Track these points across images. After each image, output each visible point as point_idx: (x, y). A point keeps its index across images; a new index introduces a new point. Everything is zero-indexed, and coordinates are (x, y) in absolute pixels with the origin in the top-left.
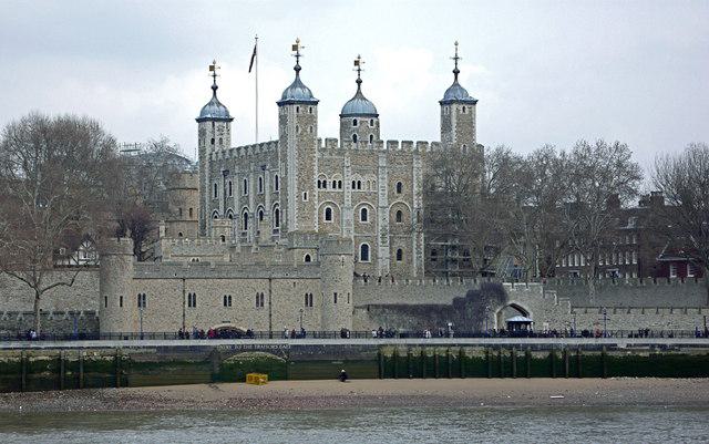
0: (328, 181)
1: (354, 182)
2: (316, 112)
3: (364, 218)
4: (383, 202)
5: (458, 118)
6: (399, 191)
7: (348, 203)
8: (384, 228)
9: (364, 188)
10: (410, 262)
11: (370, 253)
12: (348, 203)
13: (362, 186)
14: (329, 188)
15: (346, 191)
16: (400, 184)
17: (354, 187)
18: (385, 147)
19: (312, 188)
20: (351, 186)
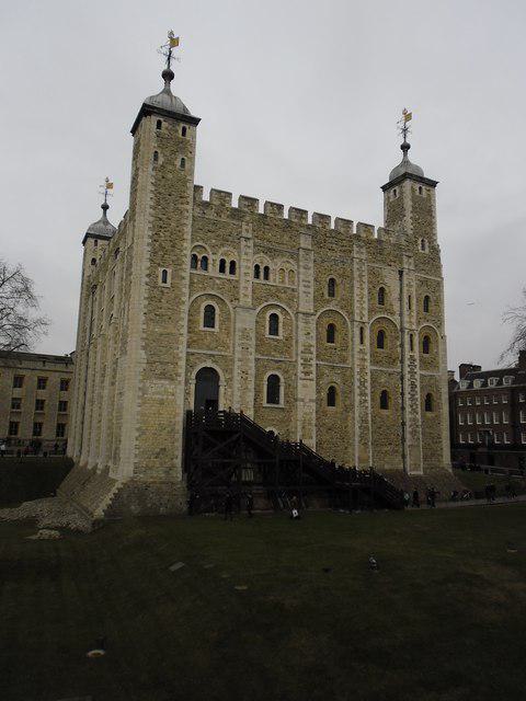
0: (211, 258)
1: (257, 267)
2: (194, 137)
3: (274, 330)
4: (306, 304)
5: (414, 199)
6: (332, 294)
7: (246, 299)
8: (307, 350)
9: (274, 279)
10: (349, 408)
11: (282, 389)
12: (246, 299)
13: (271, 276)
14: (213, 270)
15: (243, 279)
16: (332, 281)
17: (257, 275)
18: (310, 221)
19: (178, 264)
20: (252, 272)
